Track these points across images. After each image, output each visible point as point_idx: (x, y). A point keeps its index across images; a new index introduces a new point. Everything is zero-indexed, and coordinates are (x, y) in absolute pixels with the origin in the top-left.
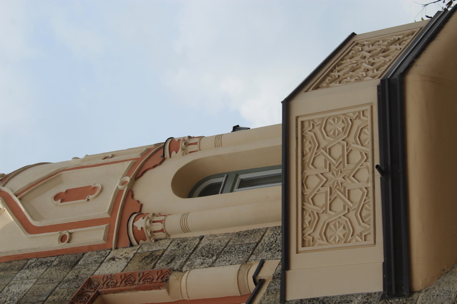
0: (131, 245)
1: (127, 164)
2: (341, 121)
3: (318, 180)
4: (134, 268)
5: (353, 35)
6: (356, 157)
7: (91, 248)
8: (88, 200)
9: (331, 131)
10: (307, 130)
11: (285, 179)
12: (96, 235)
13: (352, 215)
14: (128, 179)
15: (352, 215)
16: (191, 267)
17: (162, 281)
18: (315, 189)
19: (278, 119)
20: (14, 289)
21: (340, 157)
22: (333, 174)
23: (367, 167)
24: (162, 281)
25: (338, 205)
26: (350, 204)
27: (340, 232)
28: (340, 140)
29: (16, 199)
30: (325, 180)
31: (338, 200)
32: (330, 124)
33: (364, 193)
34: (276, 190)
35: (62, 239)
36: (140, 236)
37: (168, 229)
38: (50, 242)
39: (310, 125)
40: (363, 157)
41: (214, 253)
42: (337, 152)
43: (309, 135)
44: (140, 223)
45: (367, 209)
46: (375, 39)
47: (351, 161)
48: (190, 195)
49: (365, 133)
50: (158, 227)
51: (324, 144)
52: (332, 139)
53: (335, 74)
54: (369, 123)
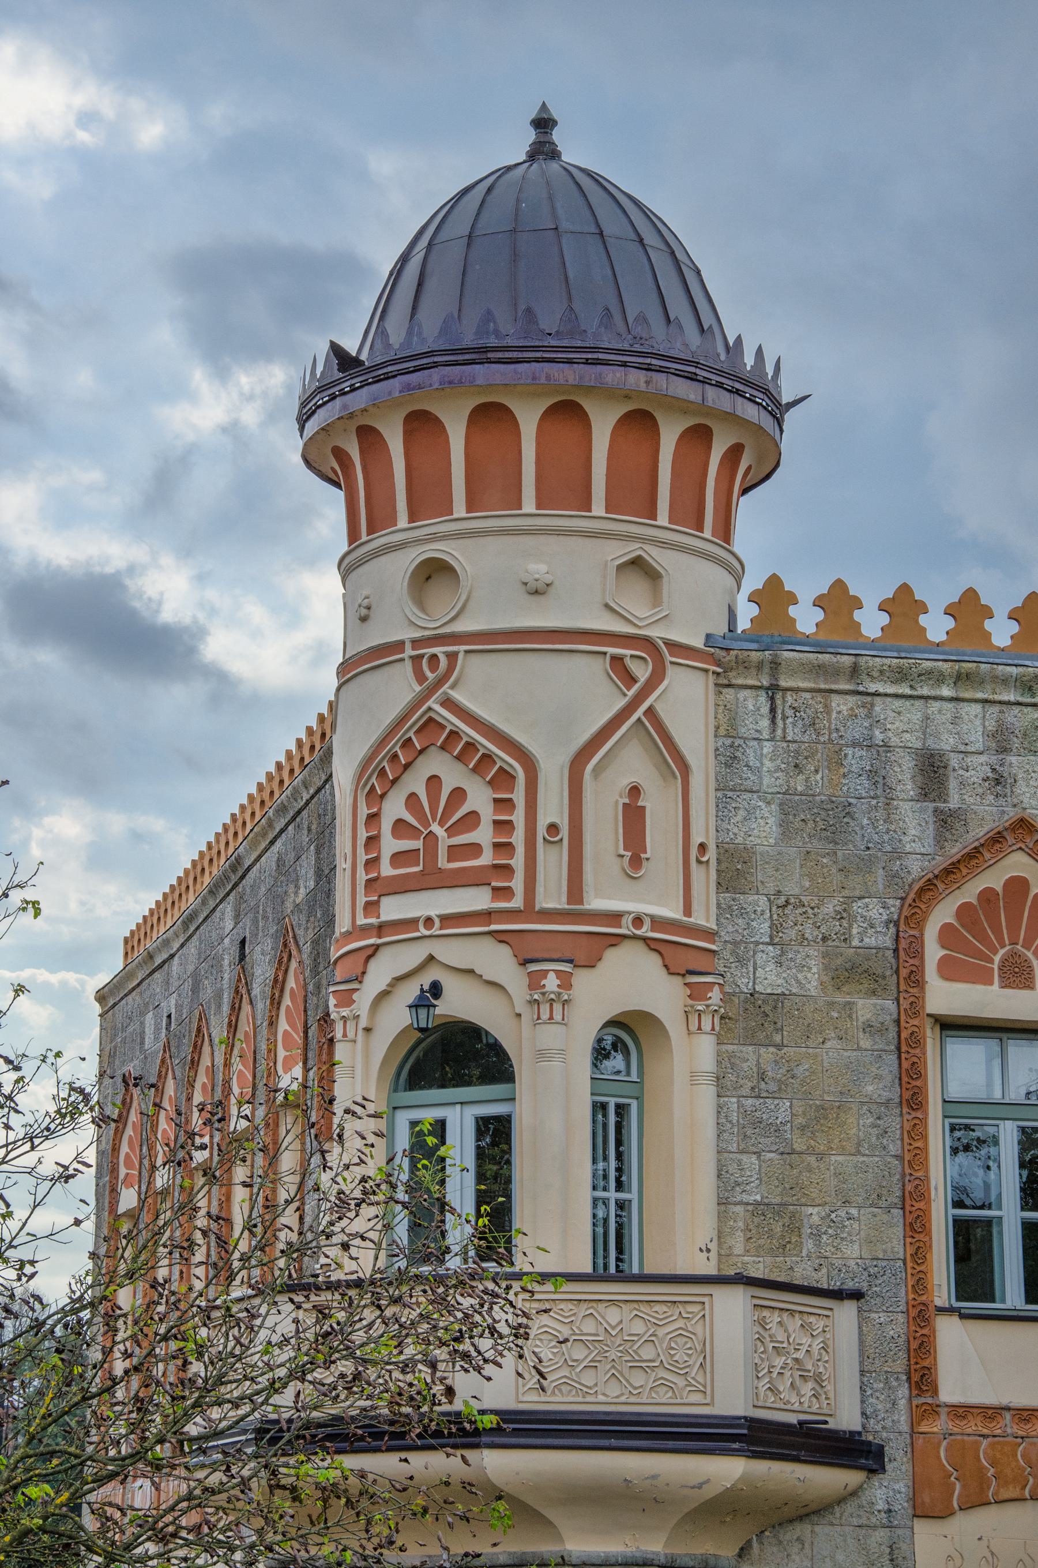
2: (686, 1359)
3: (613, 1324)
6: (638, 1379)
8: (647, 859)
9: (676, 1343)
10: (681, 1308)
13: (565, 1372)
15: (565, 1372)
18: (603, 1318)
21: (640, 1356)
22: (620, 1345)
23: (622, 1394)
25: (579, 1353)
26: (578, 1370)
28: (662, 1357)
30: (614, 1333)
31: (587, 1352)
32: (686, 1343)
33: (590, 1388)
39: (688, 1313)
40: (635, 1388)
45: (570, 1391)
47: (633, 1370)
49: (667, 1392)
51: (661, 1332)
52: (665, 1345)
54: (679, 1401)
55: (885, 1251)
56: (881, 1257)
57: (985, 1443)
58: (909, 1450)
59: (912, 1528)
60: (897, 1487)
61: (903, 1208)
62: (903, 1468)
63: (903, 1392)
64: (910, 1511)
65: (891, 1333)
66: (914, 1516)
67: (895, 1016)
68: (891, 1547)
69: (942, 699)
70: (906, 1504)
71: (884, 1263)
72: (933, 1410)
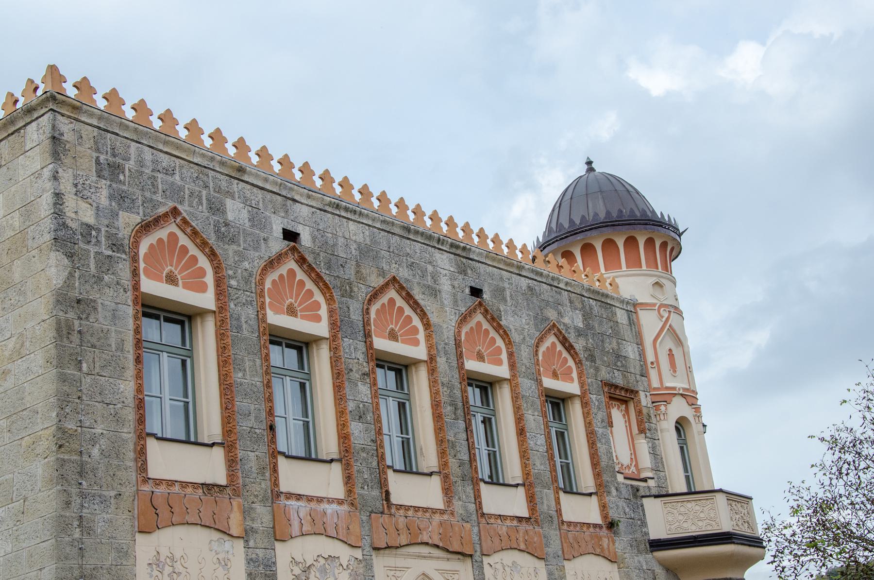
0: (653, 403)
1: (687, 386)
4: (645, 411)
5: (751, 499)
6: (700, 523)
7: (649, 381)
11: (690, 493)
12: (655, 384)
14: (681, 392)
16: (648, 442)
17: (642, 431)
19: (716, 488)
20: (630, 349)
24: (642, 431)
25: (681, 517)
27: (670, 519)
29: (668, 327)
34: (685, 490)
35: (652, 363)
36: (657, 408)
37: (662, 422)
38: (650, 357)
41: (654, 453)
42: (702, 515)
43: (708, 502)
44: (663, 408)
46: (750, 513)
48: (677, 422)
50: (662, 418)
53: (734, 503)
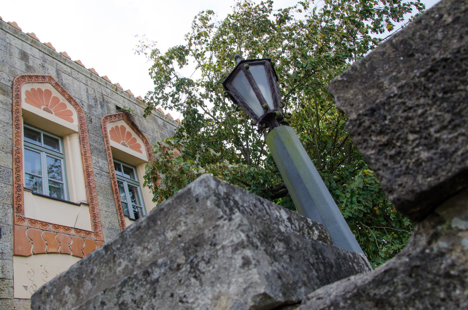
55: (4, 165)
56: (3, 165)
57: (43, 232)
58: (12, 231)
59: (13, 260)
60: (6, 244)
61: (12, 154)
62: (9, 237)
63: (10, 211)
64: (12, 254)
65: (6, 191)
66: (15, 255)
67: (11, 103)
68: (2, 267)
69: (27, 43)
70: (10, 251)
71: (4, 168)
72: (23, 219)
